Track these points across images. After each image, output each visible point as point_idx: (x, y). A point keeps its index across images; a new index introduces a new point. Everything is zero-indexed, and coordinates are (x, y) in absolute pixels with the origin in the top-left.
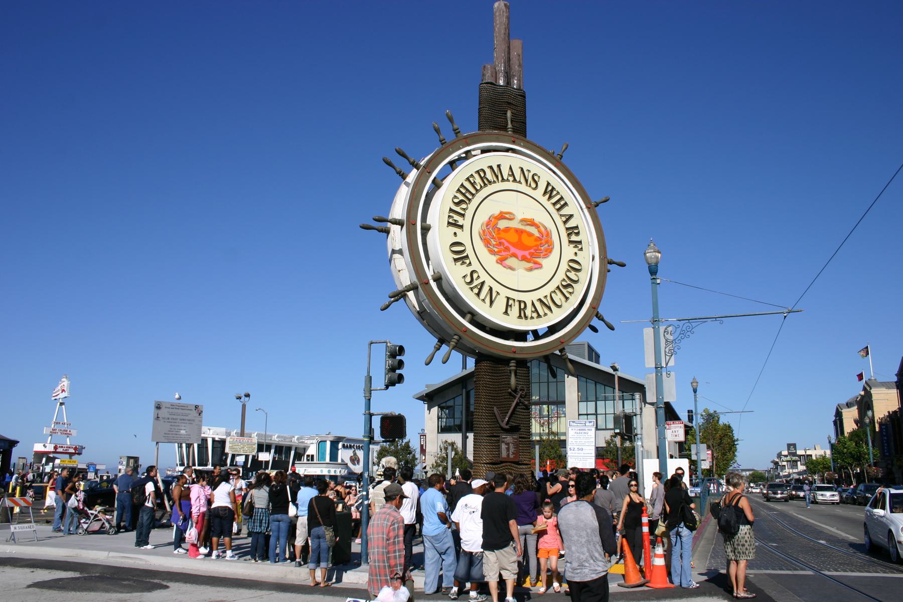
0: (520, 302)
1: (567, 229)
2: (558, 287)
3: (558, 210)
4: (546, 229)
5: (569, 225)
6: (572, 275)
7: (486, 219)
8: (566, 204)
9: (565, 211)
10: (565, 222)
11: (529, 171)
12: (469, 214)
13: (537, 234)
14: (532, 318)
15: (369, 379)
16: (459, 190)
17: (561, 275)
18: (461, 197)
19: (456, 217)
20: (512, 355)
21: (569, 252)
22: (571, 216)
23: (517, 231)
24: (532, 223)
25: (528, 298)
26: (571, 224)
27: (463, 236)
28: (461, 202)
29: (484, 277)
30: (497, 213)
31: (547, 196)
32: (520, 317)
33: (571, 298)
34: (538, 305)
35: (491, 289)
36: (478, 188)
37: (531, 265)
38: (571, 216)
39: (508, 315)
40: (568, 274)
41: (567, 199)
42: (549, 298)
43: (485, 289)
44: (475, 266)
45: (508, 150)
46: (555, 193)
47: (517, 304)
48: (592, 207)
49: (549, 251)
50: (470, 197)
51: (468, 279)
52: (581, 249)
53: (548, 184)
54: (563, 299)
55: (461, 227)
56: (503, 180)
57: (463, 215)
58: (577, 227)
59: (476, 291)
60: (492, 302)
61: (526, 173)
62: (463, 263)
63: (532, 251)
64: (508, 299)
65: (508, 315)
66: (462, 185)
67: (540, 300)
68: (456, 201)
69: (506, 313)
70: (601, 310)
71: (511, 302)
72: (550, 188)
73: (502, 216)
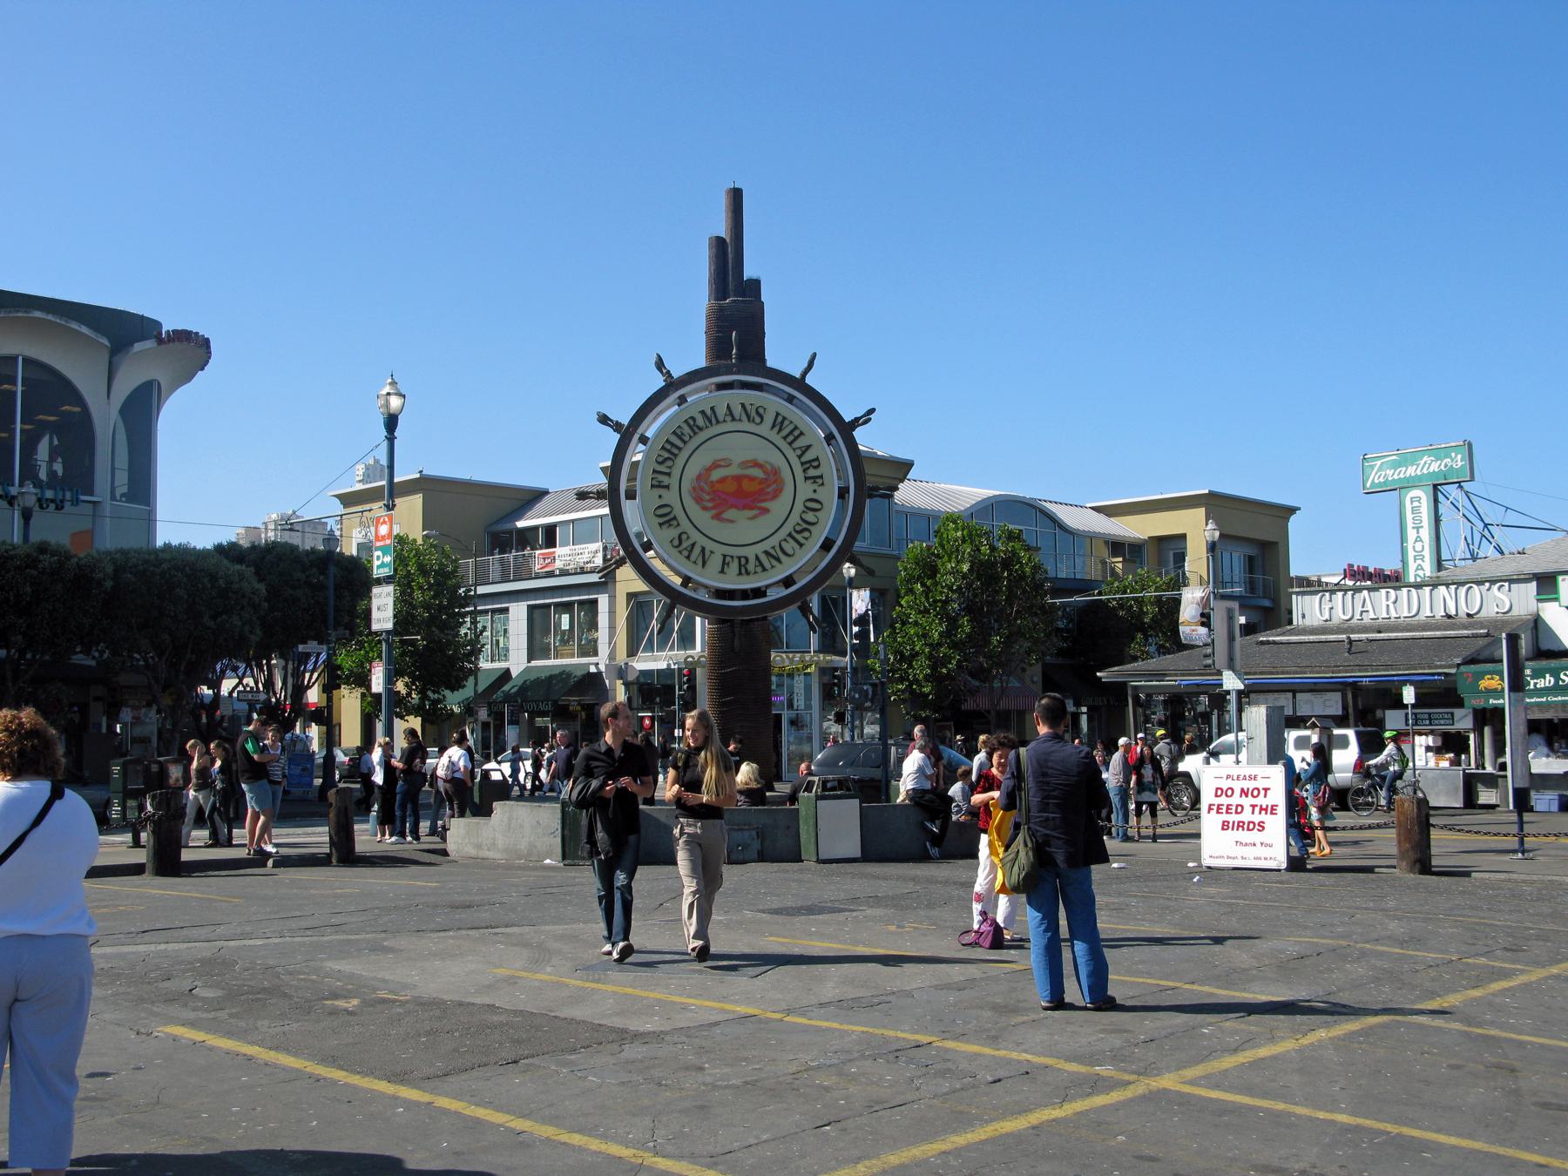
6: (810, 517)
9: (801, 442)
12: (676, 472)
16: (663, 448)
17: (795, 518)
18: (666, 455)
19: (661, 478)
21: (806, 490)
22: (808, 447)
24: (756, 464)
25: (750, 552)
26: (809, 456)
27: (671, 497)
29: (695, 536)
30: (708, 462)
35: (703, 549)
37: (755, 512)
38: (808, 447)
43: (697, 550)
44: (685, 525)
49: (776, 495)
50: (675, 451)
55: (667, 487)
58: (817, 459)
60: (704, 563)
66: (668, 441)
67: (766, 553)
69: (722, 571)
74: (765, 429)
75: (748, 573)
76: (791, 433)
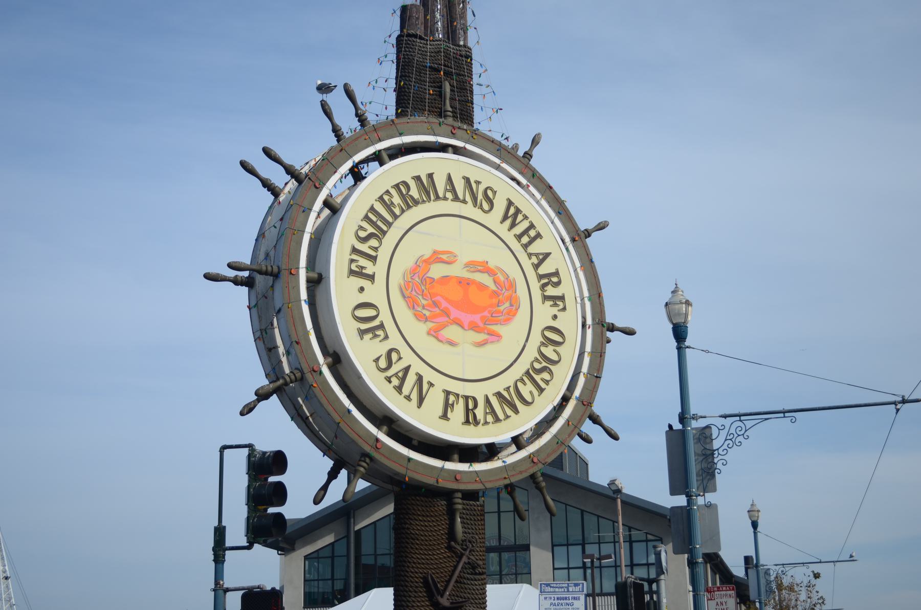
0: (467, 398)
1: (541, 277)
2: (527, 373)
3: (525, 246)
4: (507, 277)
5: (543, 270)
6: (549, 351)
7: (410, 263)
8: (538, 236)
10: (536, 267)
11: (478, 183)
13: (493, 287)
14: (486, 423)
15: (220, 533)
16: (366, 218)
17: (531, 353)
18: (371, 230)
19: (363, 262)
20: (454, 486)
21: (544, 314)
22: (547, 255)
23: (461, 282)
24: (484, 268)
25: (478, 391)
26: (544, 269)
27: (375, 293)
28: (371, 236)
29: (408, 358)
30: (428, 254)
31: (508, 222)
32: (467, 422)
33: (549, 389)
34: (494, 402)
35: (420, 378)
36: (397, 211)
38: (547, 255)
39: (448, 419)
40: (543, 349)
41: (540, 228)
42: (512, 390)
45: (443, 148)
46: (520, 217)
47: (461, 401)
48: (579, 237)
49: (511, 314)
50: (385, 228)
51: (383, 363)
52: (564, 309)
53: (510, 203)
54: (536, 393)
55: (371, 278)
56: (437, 198)
57: (373, 259)
58: (556, 274)
59: (395, 382)
61: (474, 186)
62: (376, 336)
63: (486, 313)
64: (447, 393)
65: (448, 419)
66: (372, 209)
67: (499, 395)
68: (363, 234)
69: (445, 416)
70: (597, 408)
71: (452, 398)
72: (512, 211)
73: (437, 257)
74: (494, 219)
75: (476, 423)
76: (526, 232)
